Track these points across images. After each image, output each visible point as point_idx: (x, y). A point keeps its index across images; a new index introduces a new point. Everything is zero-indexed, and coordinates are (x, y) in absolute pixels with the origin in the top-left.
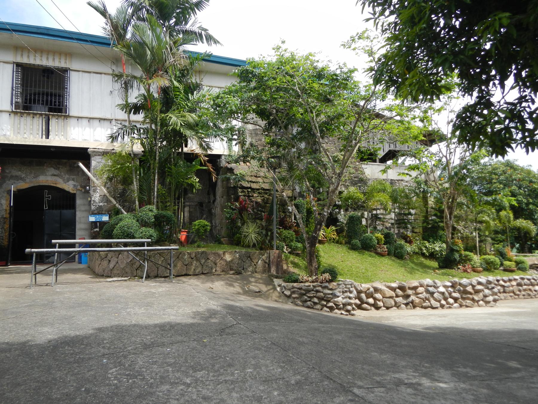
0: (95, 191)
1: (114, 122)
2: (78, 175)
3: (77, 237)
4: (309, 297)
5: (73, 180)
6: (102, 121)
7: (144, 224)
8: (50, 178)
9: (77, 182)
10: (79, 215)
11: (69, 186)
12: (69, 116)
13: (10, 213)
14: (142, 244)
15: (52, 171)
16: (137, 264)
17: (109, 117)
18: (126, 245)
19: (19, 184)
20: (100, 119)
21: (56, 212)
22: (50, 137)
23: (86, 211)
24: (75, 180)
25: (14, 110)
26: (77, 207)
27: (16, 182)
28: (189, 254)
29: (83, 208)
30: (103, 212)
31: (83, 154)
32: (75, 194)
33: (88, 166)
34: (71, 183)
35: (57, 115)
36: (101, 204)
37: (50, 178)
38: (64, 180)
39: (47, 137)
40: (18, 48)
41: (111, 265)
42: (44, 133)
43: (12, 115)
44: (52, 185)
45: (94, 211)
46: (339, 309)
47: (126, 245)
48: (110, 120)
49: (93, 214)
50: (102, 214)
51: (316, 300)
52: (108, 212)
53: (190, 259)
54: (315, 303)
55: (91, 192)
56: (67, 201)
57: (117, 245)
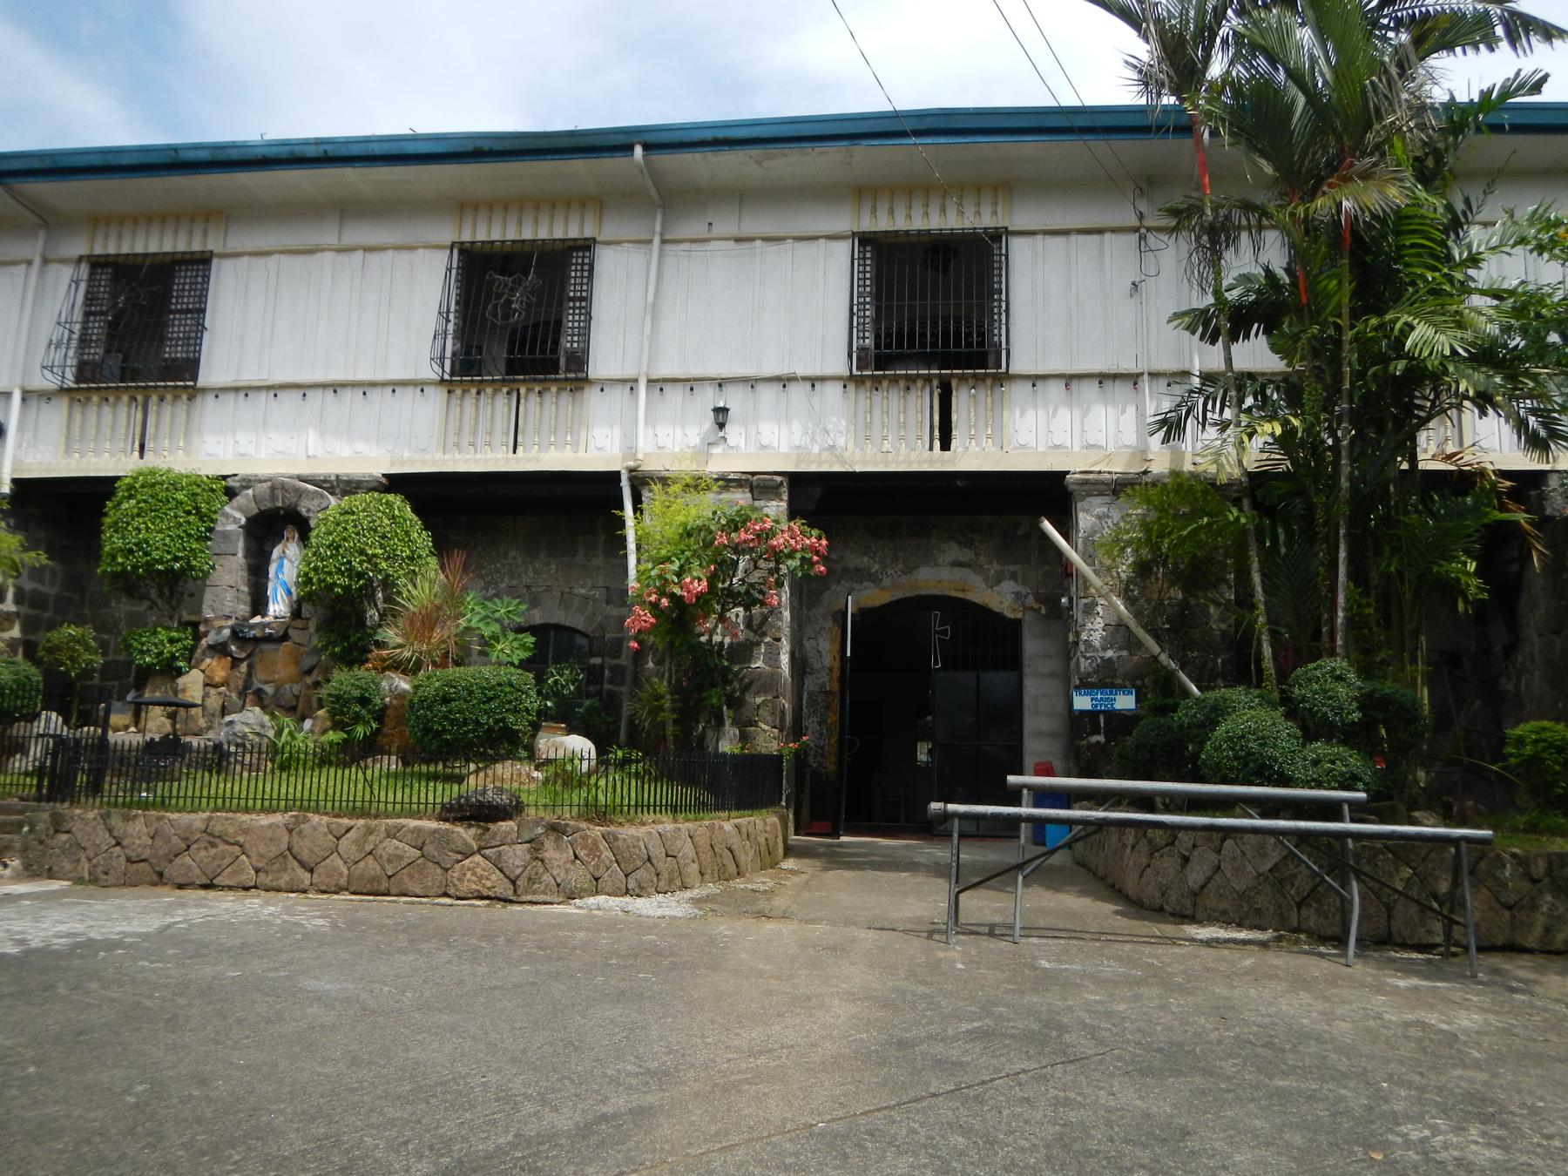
0: (1090, 610)
1: (1145, 384)
3: (1029, 760)
5: (1014, 577)
6: (1108, 384)
7: (1313, 727)
8: (949, 573)
9: (1024, 582)
10: (1033, 688)
12: (1008, 377)
13: (841, 679)
14: (1330, 810)
15: (954, 552)
16: (1303, 883)
17: (1129, 366)
19: (865, 593)
20: (1103, 378)
23: (1052, 675)
25: (855, 372)
26: (1026, 662)
27: (857, 587)
28: (1522, 862)
30: (1119, 681)
31: (1049, 493)
32: (1018, 623)
33: (1066, 530)
34: (1008, 586)
35: (974, 376)
36: (1110, 654)
37: (949, 573)
38: (986, 579)
39: (946, 446)
40: (862, 192)
41: (1195, 876)
42: (937, 433)
43: (851, 387)
44: (954, 594)
45: (1089, 675)
47: (1269, 807)
48: (1133, 378)
49: (1085, 685)
50: (1113, 686)
52: (1133, 680)
55: (1078, 614)
56: (992, 641)
57: (1269, 807)
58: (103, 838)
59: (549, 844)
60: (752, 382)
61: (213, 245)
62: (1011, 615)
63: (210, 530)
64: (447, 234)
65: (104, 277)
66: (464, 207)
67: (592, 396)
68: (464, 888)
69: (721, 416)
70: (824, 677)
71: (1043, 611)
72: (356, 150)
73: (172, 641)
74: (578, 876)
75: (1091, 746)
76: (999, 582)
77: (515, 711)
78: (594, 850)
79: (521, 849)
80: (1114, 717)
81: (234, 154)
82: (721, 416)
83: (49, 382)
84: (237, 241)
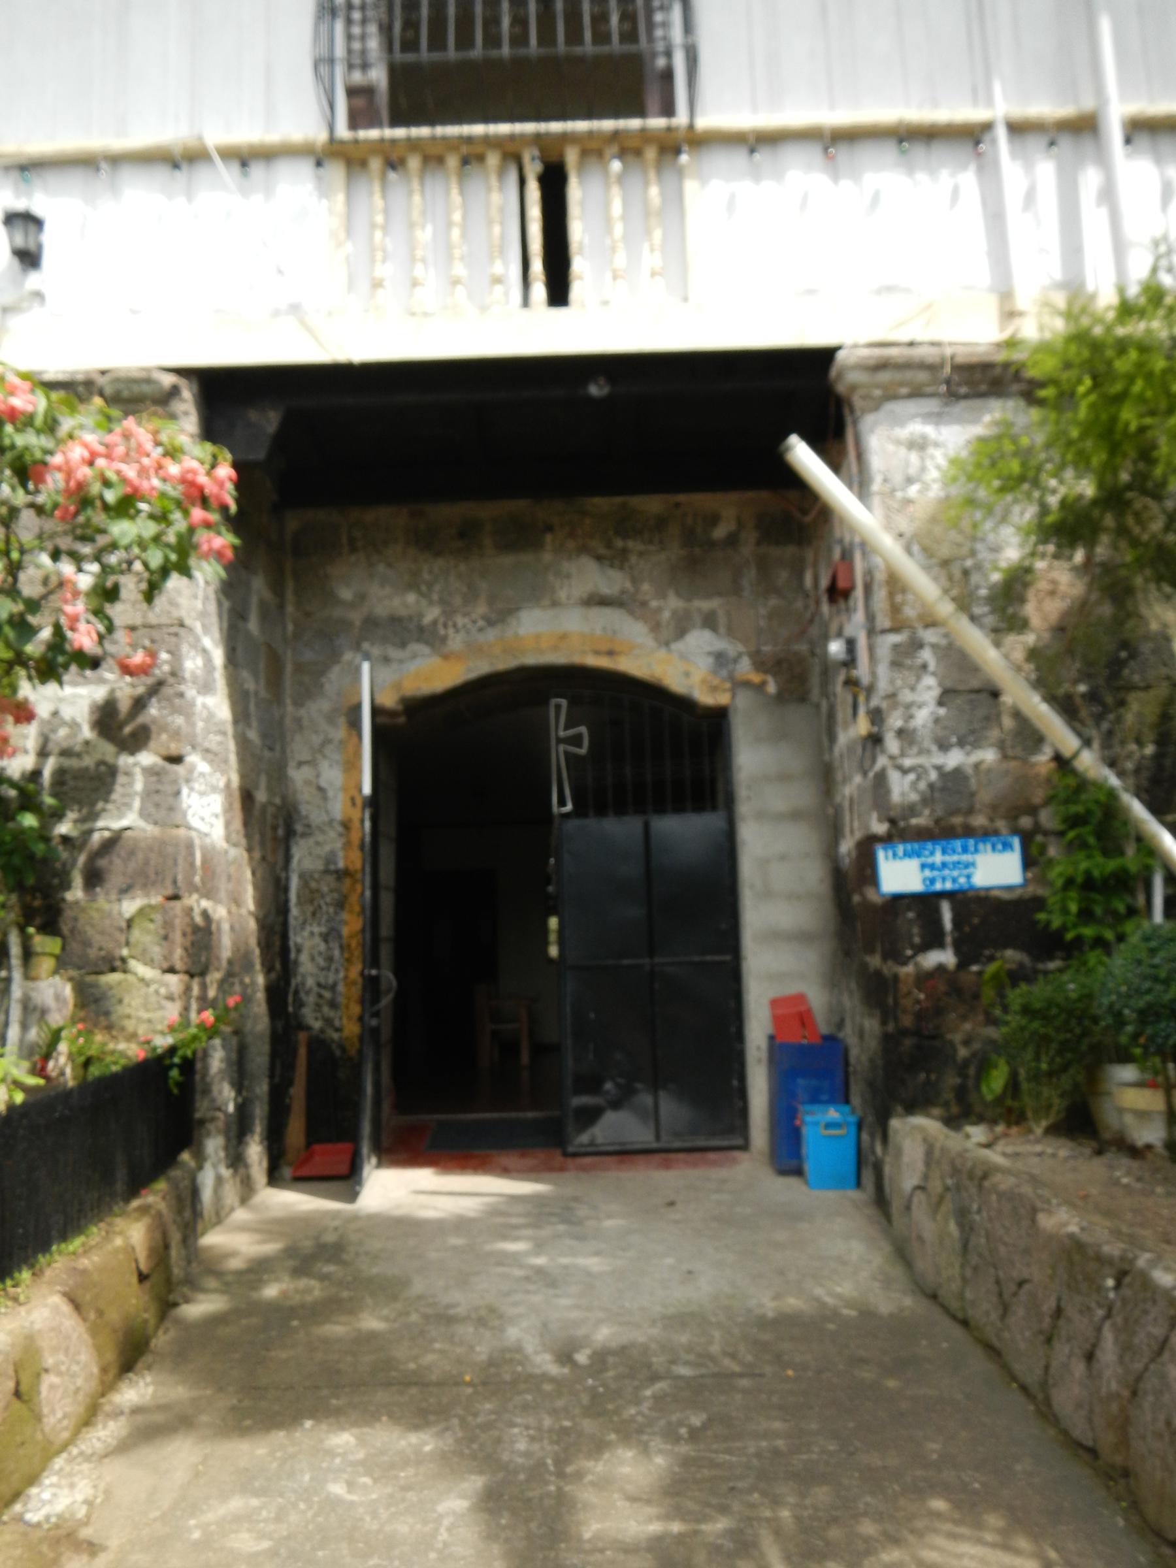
2: (737, 591)
5: (710, 622)
9: (731, 633)
11: (686, 660)
15: (589, 575)
19: (413, 667)
21: (621, 829)
22: (577, 290)
23: (795, 815)
24: (722, 620)
26: (742, 792)
27: (393, 653)
29: (779, 799)
30: (979, 821)
32: (718, 718)
34: (700, 643)
36: (954, 759)
38: (656, 628)
39: (558, 294)
43: (336, 172)
44: (592, 661)
49: (902, 832)
50: (968, 832)
52: (1013, 815)
62: (705, 698)
70: (332, 842)
71: (772, 688)
75: (925, 978)
76: (681, 632)
80: (974, 906)
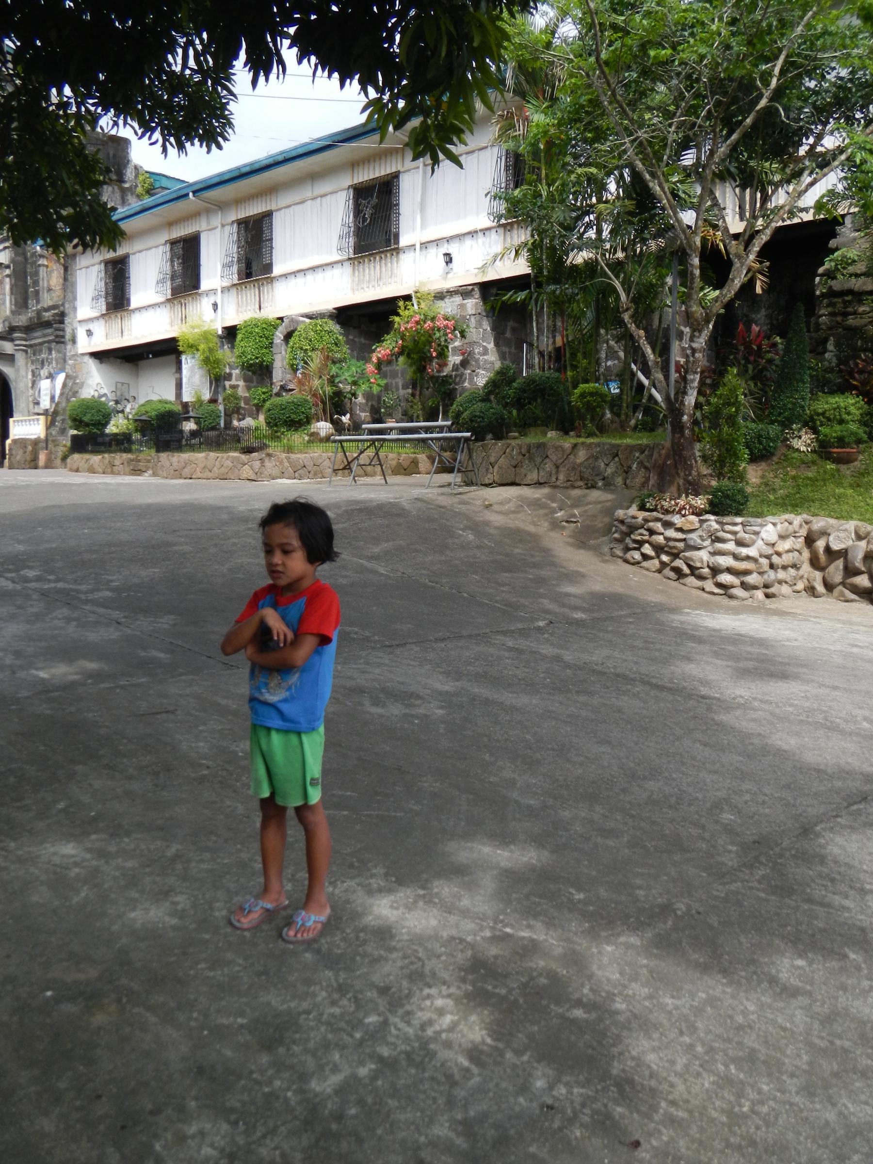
4: (635, 541)
18: (427, 430)
46: (701, 578)
51: (647, 549)
53: (520, 457)
54: (645, 557)
58: (168, 463)
59: (267, 460)
60: (460, 237)
61: (273, 208)
63: (272, 343)
64: (347, 180)
65: (247, 229)
66: (354, 165)
67: (402, 256)
68: (245, 476)
69: (449, 259)
72: (294, 154)
73: (264, 393)
74: (276, 472)
77: (295, 413)
78: (281, 462)
79: (258, 463)
81: (257, 166)
82: (449, 259)
83: (226, 283)
84: (284, 199)
